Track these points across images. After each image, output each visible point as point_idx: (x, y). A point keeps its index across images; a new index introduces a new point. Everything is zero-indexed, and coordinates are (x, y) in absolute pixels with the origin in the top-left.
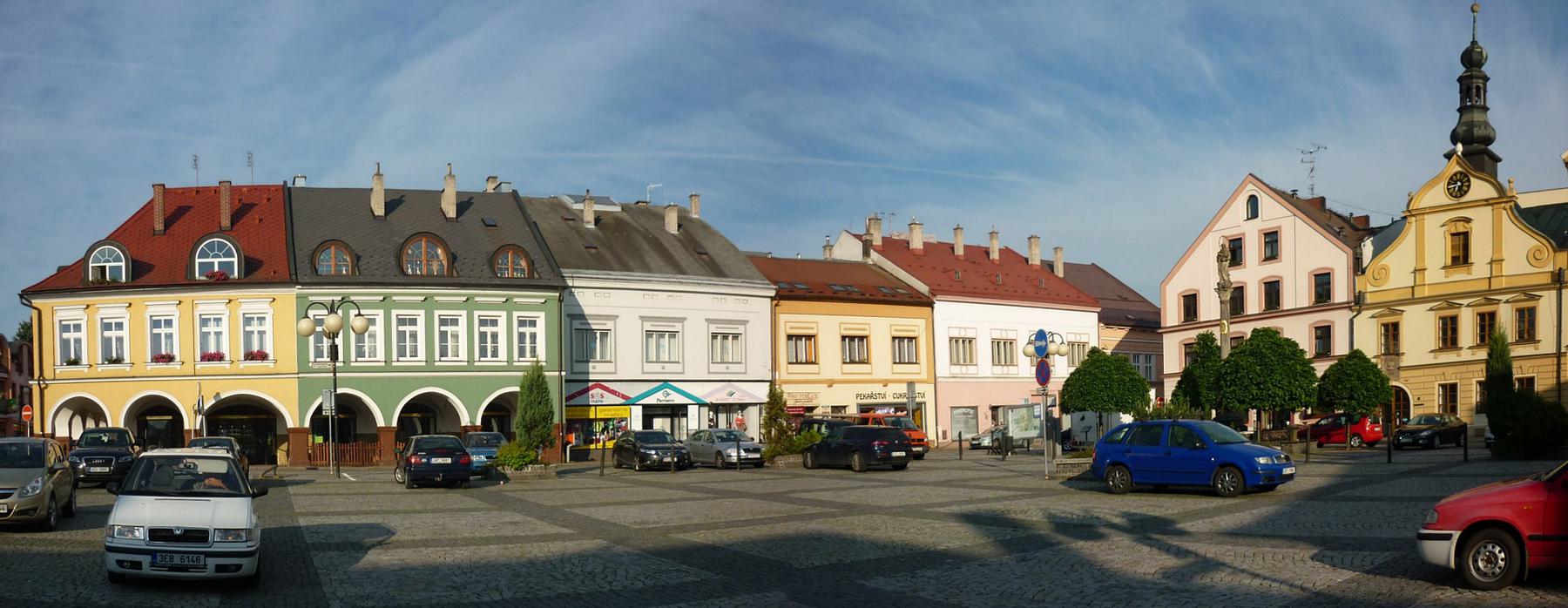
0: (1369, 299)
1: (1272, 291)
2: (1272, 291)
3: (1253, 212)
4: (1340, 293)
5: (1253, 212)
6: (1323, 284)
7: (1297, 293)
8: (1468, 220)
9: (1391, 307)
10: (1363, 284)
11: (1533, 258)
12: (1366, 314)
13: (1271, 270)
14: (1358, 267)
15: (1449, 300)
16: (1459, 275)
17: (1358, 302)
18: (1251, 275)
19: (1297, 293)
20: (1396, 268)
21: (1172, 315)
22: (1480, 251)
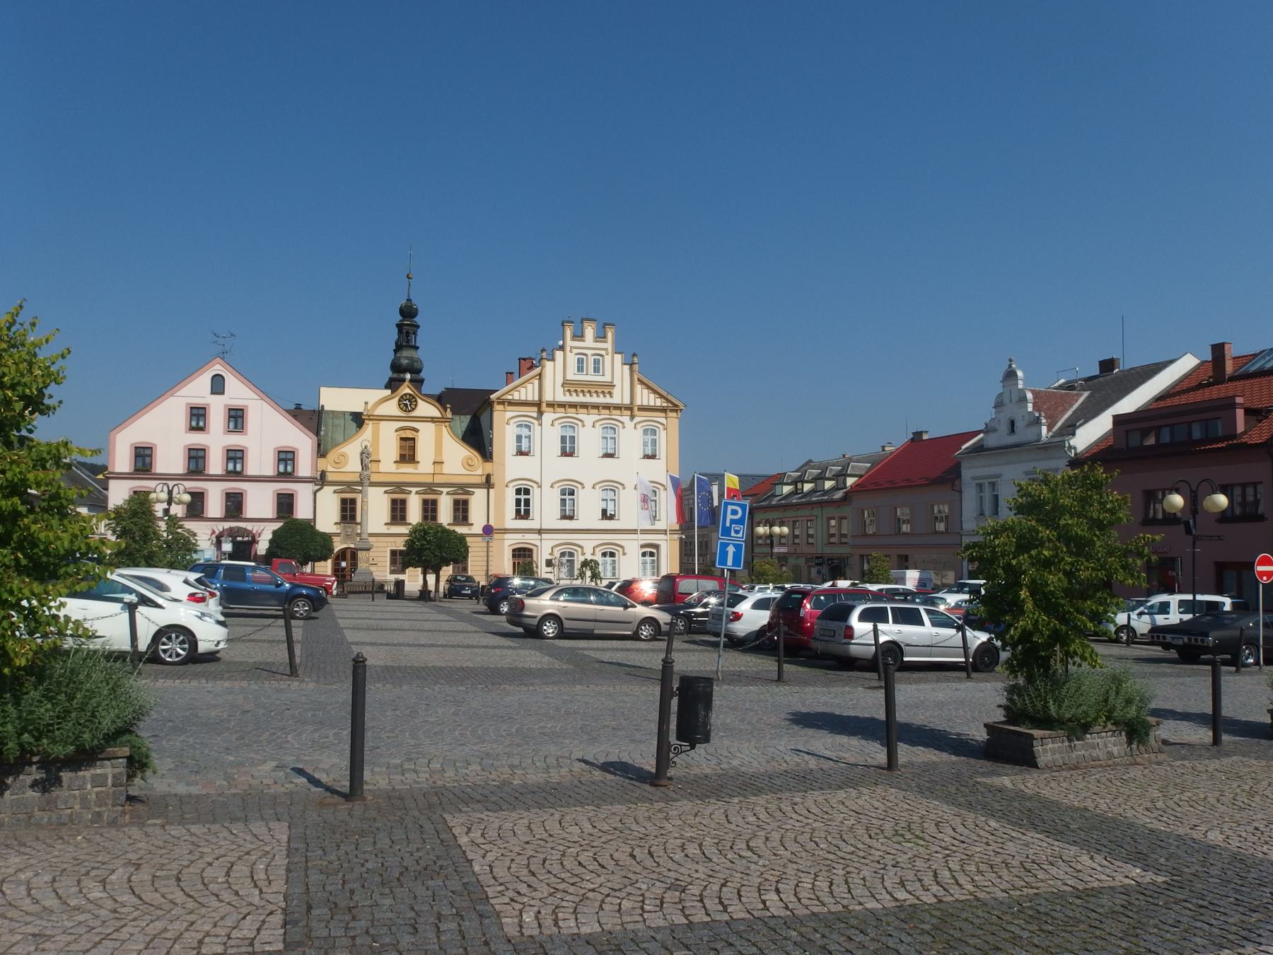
0: (330, 477)
1: (235, 456)
2: (235, 456)
3: (218, 385)
4: (304, 467)
5: (218, 385)
6: (286, 457)
7: (260, 462)
8: (416, 430)
9: (349, 486)
10: (323, 464)
11: (468, 464)
12: (328, 490)
13: (235, 440)
14: (321, 452)
15: (399, 487)
16: (407, 468)
17: (321, 480)
18: (216, 440)
19: (260, 462)
20: (347, 459)
21: (122, 461)
22: (425, 451)
